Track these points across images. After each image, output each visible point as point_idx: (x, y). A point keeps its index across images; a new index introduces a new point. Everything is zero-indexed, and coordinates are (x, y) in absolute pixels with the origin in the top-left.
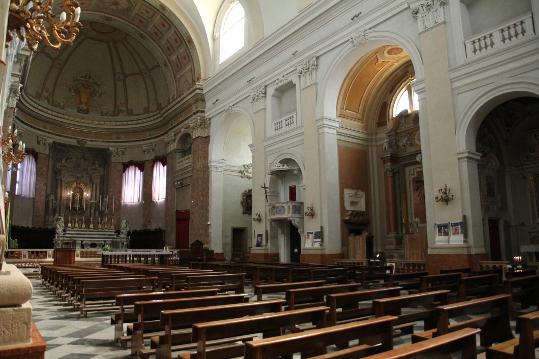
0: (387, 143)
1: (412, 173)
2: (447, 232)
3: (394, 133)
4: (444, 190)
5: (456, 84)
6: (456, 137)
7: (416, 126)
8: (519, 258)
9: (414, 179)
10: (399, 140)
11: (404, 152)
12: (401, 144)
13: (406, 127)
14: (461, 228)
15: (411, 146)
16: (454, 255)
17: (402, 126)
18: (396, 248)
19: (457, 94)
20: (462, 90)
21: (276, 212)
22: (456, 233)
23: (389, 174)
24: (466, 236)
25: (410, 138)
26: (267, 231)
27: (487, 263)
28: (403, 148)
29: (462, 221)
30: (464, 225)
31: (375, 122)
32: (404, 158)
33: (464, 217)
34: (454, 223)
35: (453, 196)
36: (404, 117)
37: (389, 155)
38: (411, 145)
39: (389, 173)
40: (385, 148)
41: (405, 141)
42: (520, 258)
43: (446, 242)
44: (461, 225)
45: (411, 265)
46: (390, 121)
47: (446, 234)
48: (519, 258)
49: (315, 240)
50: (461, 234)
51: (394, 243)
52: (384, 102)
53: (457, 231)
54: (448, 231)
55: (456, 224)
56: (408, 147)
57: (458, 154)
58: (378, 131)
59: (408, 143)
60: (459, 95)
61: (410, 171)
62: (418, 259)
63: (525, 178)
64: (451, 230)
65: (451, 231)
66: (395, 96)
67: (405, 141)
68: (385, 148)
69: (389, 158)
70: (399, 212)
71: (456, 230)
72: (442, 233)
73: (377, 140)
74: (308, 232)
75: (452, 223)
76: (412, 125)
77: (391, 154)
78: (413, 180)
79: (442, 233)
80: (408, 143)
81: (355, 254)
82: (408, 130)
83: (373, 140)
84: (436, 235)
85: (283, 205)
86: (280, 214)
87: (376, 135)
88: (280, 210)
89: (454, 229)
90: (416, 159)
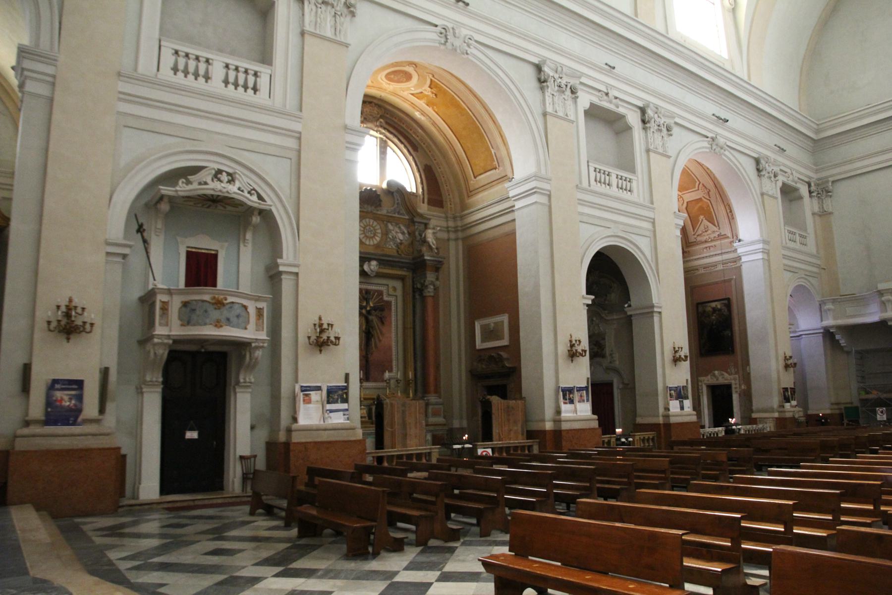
4: (63, 309)
19: (580, 221)
21: (228, 319)
49: (329, 407)
55: (580, 389)
64: (576, 396)
71: (581, 396)
74: (329, 385)
75: (577, 387)
81: (405, 436)
86: (237, 326)
88: (238, 316)
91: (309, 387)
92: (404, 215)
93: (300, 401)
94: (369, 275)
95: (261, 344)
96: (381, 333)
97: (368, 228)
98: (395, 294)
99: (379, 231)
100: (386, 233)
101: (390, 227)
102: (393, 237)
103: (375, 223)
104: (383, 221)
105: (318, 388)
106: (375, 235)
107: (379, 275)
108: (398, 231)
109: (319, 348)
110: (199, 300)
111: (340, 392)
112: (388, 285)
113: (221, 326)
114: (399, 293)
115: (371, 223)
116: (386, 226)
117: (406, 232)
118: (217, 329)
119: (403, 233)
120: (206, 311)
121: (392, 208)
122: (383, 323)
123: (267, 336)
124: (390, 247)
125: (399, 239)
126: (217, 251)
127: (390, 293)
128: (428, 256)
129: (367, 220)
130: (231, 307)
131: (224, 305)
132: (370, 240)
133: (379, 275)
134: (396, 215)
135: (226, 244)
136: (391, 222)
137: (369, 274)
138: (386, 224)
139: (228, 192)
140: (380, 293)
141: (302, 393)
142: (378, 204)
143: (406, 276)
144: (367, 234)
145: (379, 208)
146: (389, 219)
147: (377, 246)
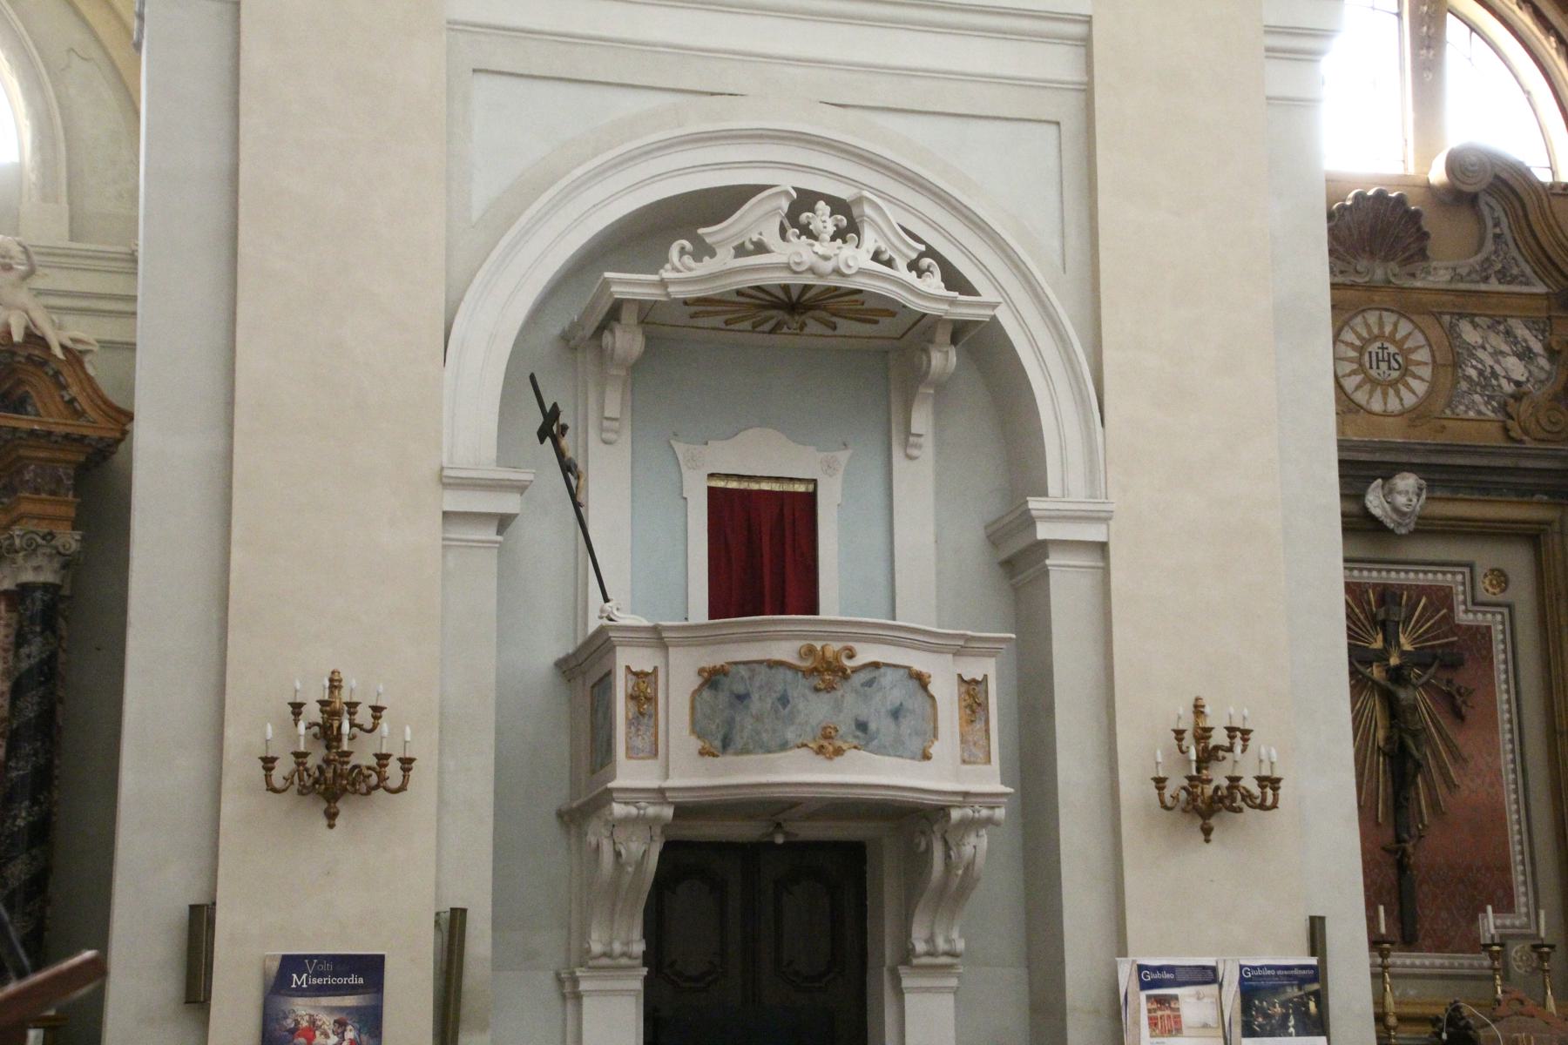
21: (862, 726)
26: (453, 925)
85: (919, 661)
86: (895, 748)
88: (896, 714)
91: (1171, 969)
92: (1527, 284)
93: (1137, 1023)
94: (1391, 531)
95: (985, 813)
96: (1457, 756)
97: (1374, 347)
98: (1500, 598)
99: (1423, 355)
100: (1453, 359)
101: (1470, 334)
102: (1481, 373)
103: (1405, 327)
104: (1437, 316)
105: (1207, 976)
106: (1405, 371)
107: (1427, 528)
108: (1505, 348)
109: (1199, 822)
110: (760, 662)
111: (1293, 992)
112: (1471, 566)
113: (839, 752)
114: (1522, 593)
115: (1388, 329)
116: (1452, 333)
117: (1537, 347)
118: (820, 761)
119: (1526, 355)
120: (784, 700)
121: (1479, 257)
122: (1459, 716)
123: (1003, 783)
124: (1472, 414)
126: (815, 481)
127: (1482, 596)
129: (1372, 318)
130: (869, 683)
131: (843, 673)
132: (1385, 395)
133: (1427, 528)
134: (1494, 285)
135: (843, 456)
136: (1471, 317)
137: (1392, 526)
138: (1452, 326)
139: (837, 272)
140: (1442, 598)
141: (1143, 995)
142: (1414, 247)
143: (1549, 523)
144: (1373, 373)
147: (1416, 415)
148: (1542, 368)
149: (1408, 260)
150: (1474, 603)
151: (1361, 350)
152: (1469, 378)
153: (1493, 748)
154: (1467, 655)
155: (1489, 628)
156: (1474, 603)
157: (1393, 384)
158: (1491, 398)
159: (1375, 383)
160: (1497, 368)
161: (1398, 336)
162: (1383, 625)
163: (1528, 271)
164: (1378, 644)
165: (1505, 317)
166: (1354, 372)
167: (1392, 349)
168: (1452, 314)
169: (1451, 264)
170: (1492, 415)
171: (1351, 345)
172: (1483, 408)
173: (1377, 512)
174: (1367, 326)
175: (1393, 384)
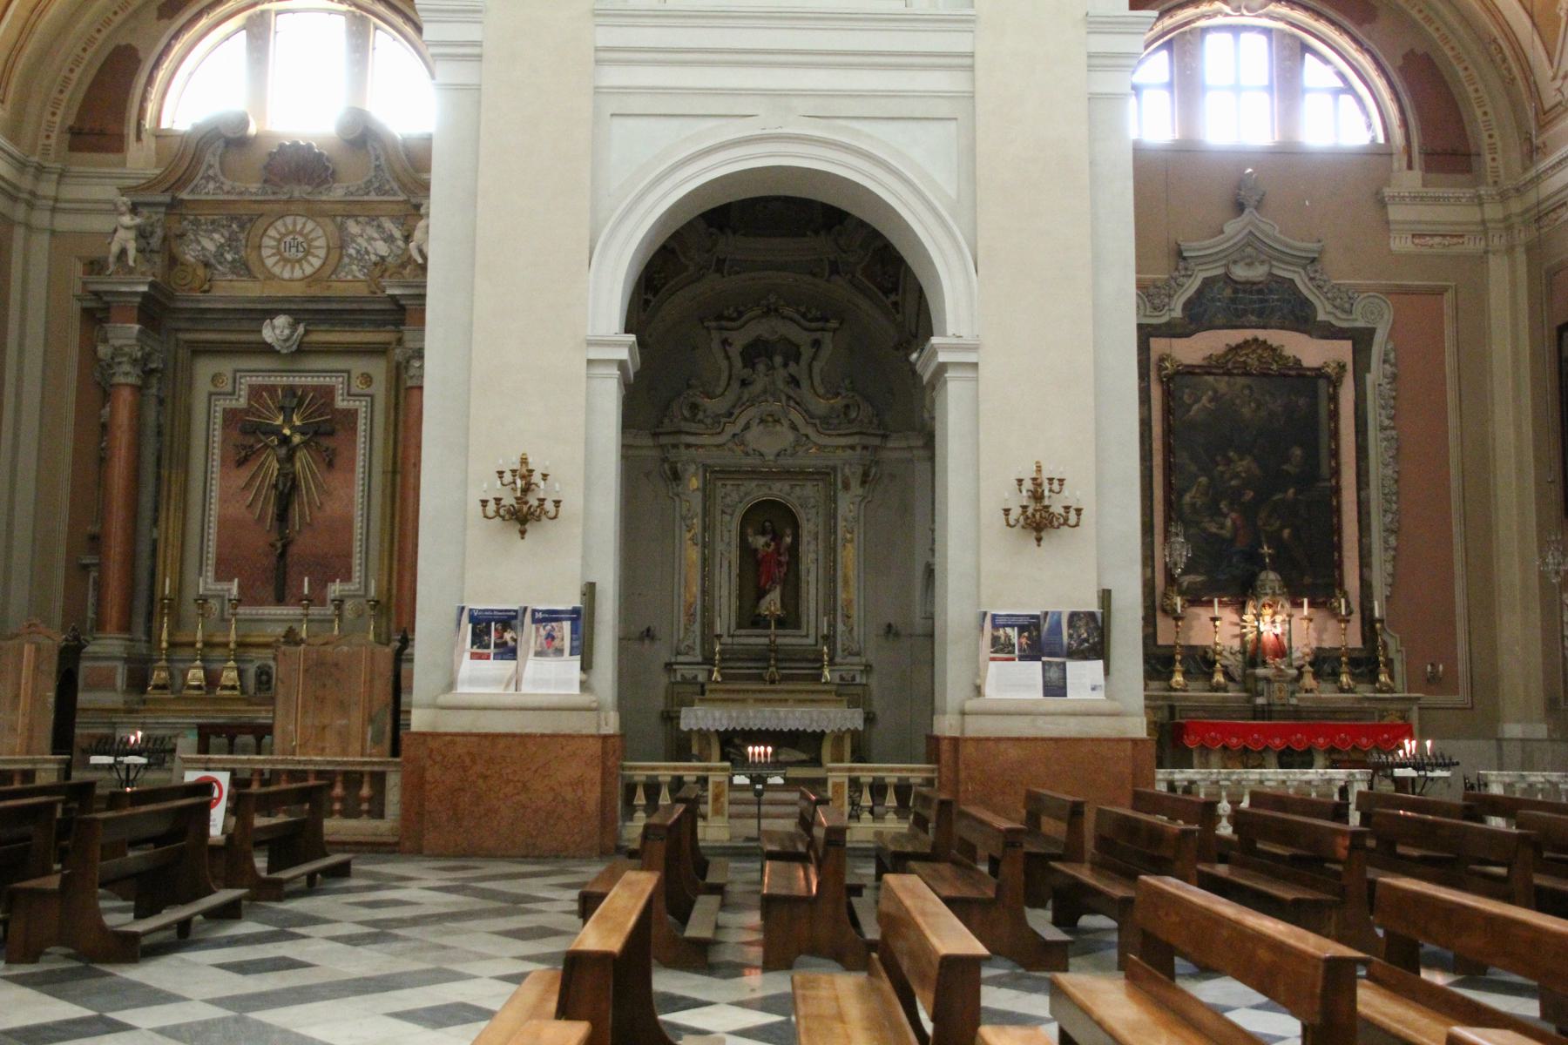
0: (131, 234)
1: (229, 388)
2: (511, 643)
3: (166, 198)
5: (614, 76)
6: (591, 275)
7: (272, 198)
8: (766, 754)
9: (231, 416)
10: (181, 236)
11: (205, 292)
12: (190, 254)
13: (226, 188)
14: (574, 631)
15: (238, 274)
16: (543, 736)
17: (208, 178)
18: (126, 703)
19: (612, 115)
20: (636, 104)
22: (549, 647)
23: (127, 374)
24: (586, 667)
25: (237, 240)
27: (653, 769)
28: (201, 272)
29: (578, 605)
30: (582, 619)
31: (58, 119)
32: (200, 316)
33: (590, 591)
34: (544, 612)
35: (557, 503)
36: (221, 143)
37: (144, 288)
38: (243, 268)
39: (126, 368)
40: (123, 252)
41: (211, 247)
42: (769, 749)
43: (508, 685)
44: (572, 620)
45: (339, 778)
46: (144, 136)
47: (508, 652)
48: (766, 754)
50: (571, 654)
51: (120, 681)
52: (123, 43)
53: (557, 643)
54: (515, 640)
55: (552, 616)
56: (224, 274)
57: (591, 343)
58: (75, 169)
59: (229, 257)
60: (617, 121)
61: (215, 378)
62: (344, 752)
63: (676, 476)
64: (530, 636)
65: (528, 642)
66: (187, 37)
67: (211, 247)
68: (123, 252)
69: (139, 299)
70: (144, 549)
71: (550, 637)
72: (488, 647)
73: (58, 205)
75: (534, 611)
76: (254, 187)
77: (152, 285)
78: (224, 420)
79: (488, 647)
80: (229, 257)
82: (234, 202)
83: (38, 203)
84: (461, 656)
87: (59, 183)
89: (543, 633)
90: (260, 332)
92: (395, 194)
94: (278, 352)
97: (288, 239)
99: (321, 242)
101: (353, 228)
102: (358, 252)
103: (310, 225)
106: (307, 252)
107: (302, 350)
108: (376, 235)
112: (349, 372)
115: (298, 228)
116: (342, 228)
117: (397, 234)
124: (350, 278)
125: (376, 255)
127: (354, 390)
128: (391, 287)
129: (289, 220)
132: (293, 268)
133: (302, 350)
134: (373, 197)
137: (278, 348)
138: (342, 223)
140: (329, 392)
144: (287, 255)
145: (322, 189)
146: (355, 209)
148: (399, 247)
149: (319, 185)
150: (349, 395)
151: (279, 241)
152: (350, 256)
153: (350, 484)
154: (338, 427)
155: (356, 410)
156: (349, 395)
157: (299, 261)
158: (363, 267)
159: (286, 261)
160: (369, 248)
161: (305, 231)
162: (282, 409)
163: (396, 187)
164: (279, 421)
165: (377, 217)
166: (274, 255)
167: (300, 239)
168: (343, 216)
169: (345, 185)
170: (362, 277)
171: (273, 238)
172: (358, 274)
173: (269, 340)
174: (285, 225)
175: (299, 261)
